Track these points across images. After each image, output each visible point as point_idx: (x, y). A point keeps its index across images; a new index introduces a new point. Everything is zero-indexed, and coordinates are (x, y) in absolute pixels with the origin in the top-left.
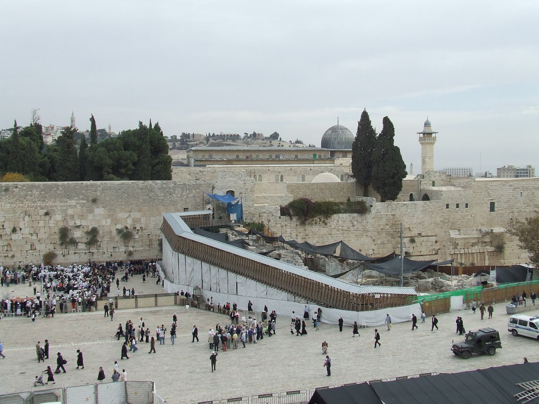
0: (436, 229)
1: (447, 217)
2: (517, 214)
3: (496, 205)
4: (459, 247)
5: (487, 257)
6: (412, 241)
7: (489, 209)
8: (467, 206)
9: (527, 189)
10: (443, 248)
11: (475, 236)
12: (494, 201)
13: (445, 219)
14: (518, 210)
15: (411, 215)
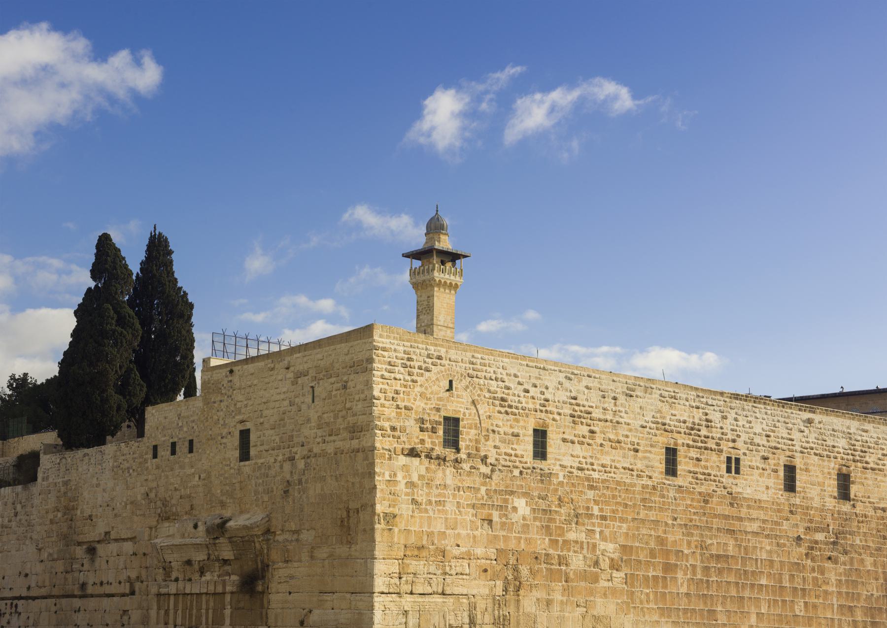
0: (136, 518)
1: (154, 485)
2: (301, 464)
3: (253, 437)
4: (174, 575)
5: (228, 612)
6: (92, 551)
7: (237, 454)
8: (191, 451)
9: (327, 372)
10: (144, 573)
11: (198, 541)
12: (248, 425)
13: (151, 490)
14: (305, 452)
15: (95, 481)
